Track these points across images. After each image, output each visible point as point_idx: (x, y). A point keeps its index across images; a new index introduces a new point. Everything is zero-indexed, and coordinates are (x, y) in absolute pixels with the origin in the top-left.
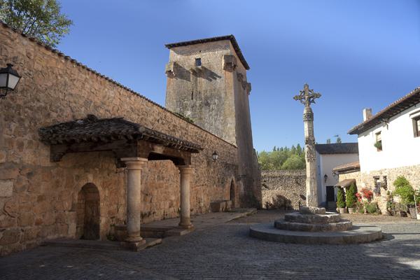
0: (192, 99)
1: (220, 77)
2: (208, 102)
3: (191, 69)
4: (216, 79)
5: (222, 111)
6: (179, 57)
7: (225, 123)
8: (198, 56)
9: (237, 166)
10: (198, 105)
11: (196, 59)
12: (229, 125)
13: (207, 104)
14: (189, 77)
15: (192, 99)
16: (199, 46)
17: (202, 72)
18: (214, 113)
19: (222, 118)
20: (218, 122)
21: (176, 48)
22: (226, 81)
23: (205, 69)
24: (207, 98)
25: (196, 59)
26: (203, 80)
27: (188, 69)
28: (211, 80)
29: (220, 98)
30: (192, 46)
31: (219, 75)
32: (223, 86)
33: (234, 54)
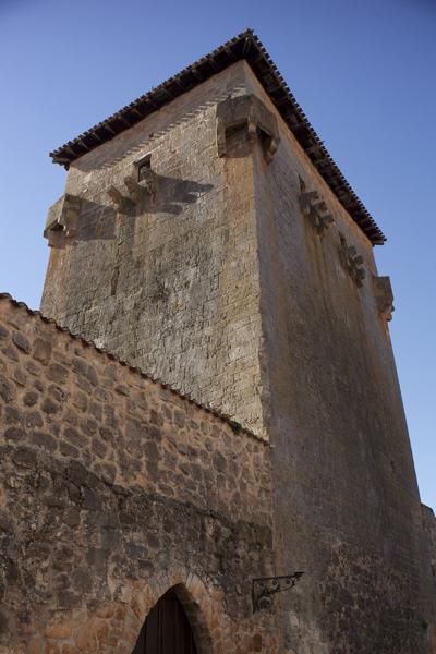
0: (113, 293)
1: (210, 187)
2: (161, 288)
3: (113, 193)
4: (192, 199)
5: (211, 306)
6: (88, 178)
7: (218, 349)
8: (140, 155)
9: (260, 537)
10: (128, 306)
12: (233, 356)
13: (161, 295)
14: (112, 225)
15: (113, 293)
16: (148, 122)
17: (157, 191)
18: (180, 319)
19: (208, 331)
20: (192, 351)
21: (85, 158)
22: (232, 190)
23: (162, 180)
24: (161, 272)
26: (152, 217)
27: (107, 202)
28: (177, 210)
29: (207, 257)
31: (204, 182)
32: (217, 212)
33: (257, 89)
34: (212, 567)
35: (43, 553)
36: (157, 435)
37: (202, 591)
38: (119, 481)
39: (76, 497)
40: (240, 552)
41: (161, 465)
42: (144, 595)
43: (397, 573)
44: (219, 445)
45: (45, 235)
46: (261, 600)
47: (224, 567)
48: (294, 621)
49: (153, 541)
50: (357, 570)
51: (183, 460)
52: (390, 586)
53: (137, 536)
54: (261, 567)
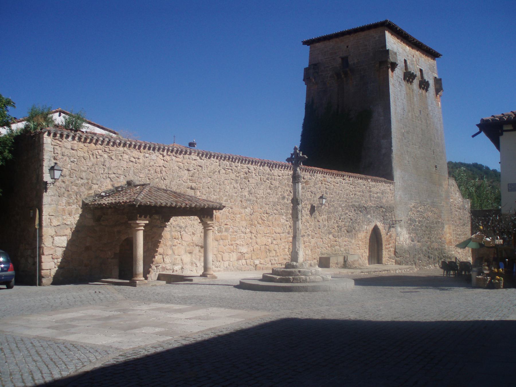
9: (390, 209)
11: (343, 59)
25: (343, 59)
30: (337, 39)
34: (382, 219)
35: (356, 223)
36: (371, 192)
37: (380, 225)
38: (365, 206)
39: (360, 211)
40: (387, 214)
41: (372, 199)
42: (371, 227)
43: (433, 209)
44: (383, 188)
45: (304, 80)
46: (392, 226)
47: (384, 219)
48: (399, 229)
49: (371, 217)
50: (419, 211)
51: (376, 195)
52: (430, 214)
53: (369, 216)
54: (392, 218)
